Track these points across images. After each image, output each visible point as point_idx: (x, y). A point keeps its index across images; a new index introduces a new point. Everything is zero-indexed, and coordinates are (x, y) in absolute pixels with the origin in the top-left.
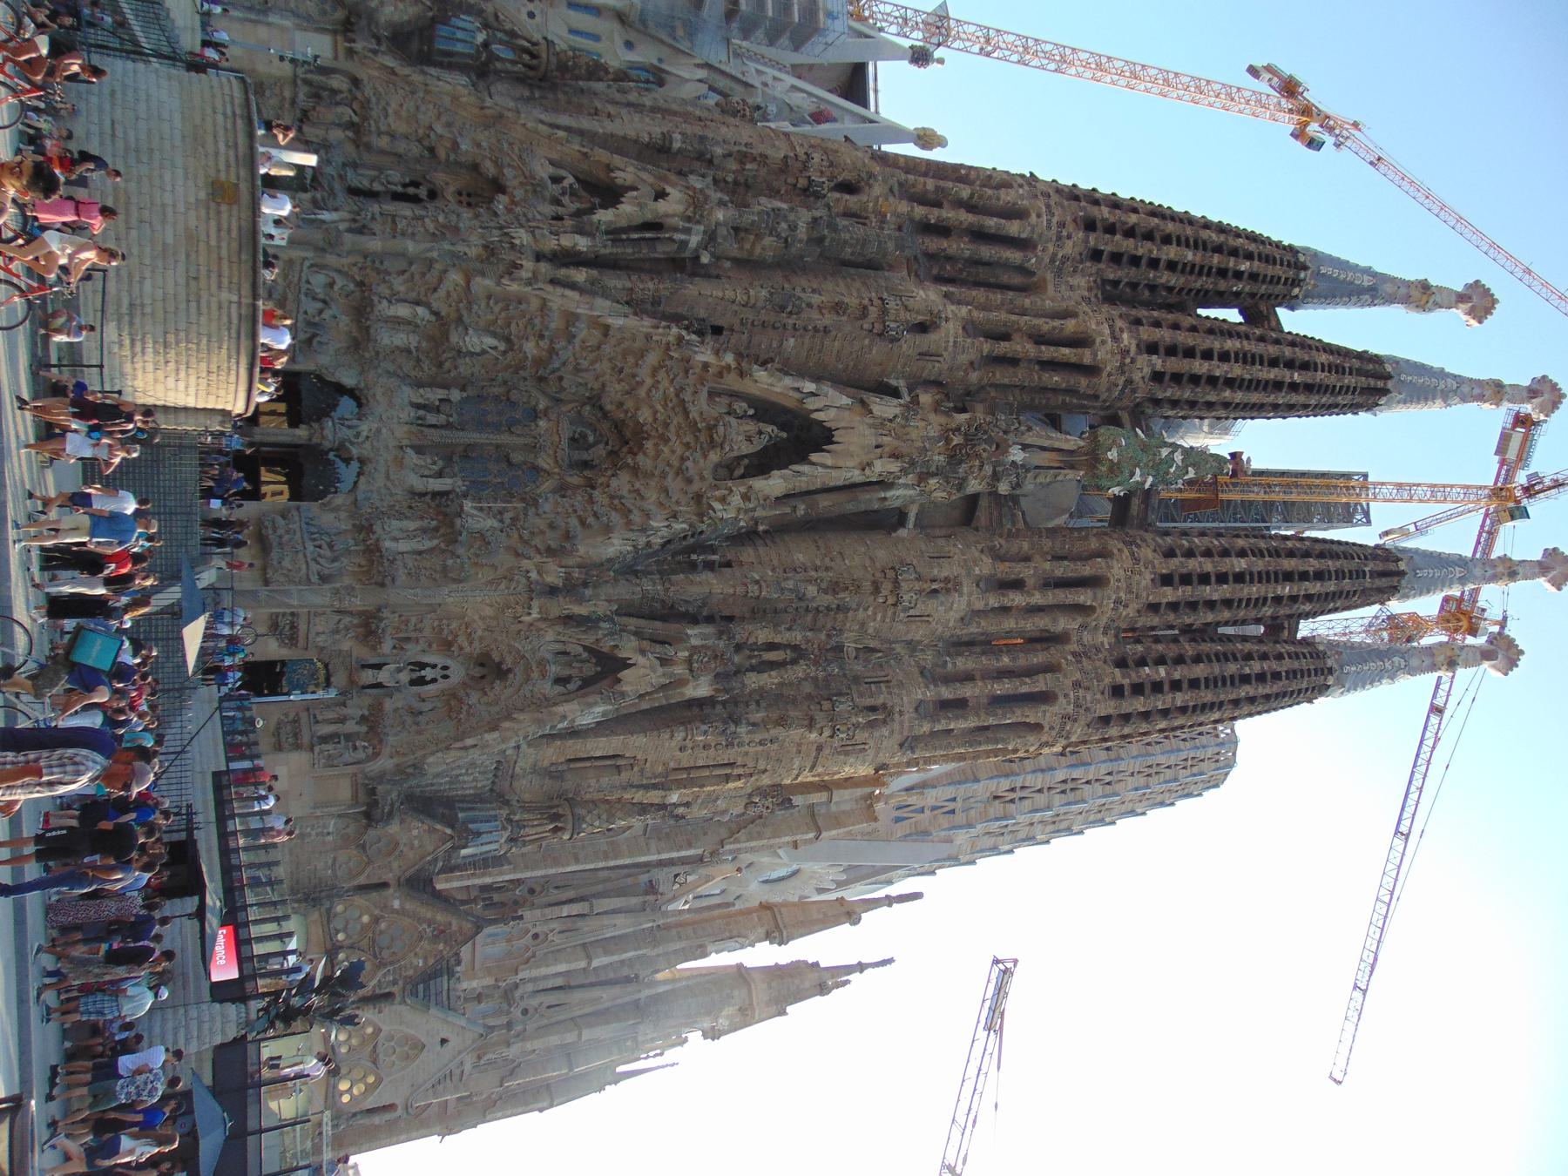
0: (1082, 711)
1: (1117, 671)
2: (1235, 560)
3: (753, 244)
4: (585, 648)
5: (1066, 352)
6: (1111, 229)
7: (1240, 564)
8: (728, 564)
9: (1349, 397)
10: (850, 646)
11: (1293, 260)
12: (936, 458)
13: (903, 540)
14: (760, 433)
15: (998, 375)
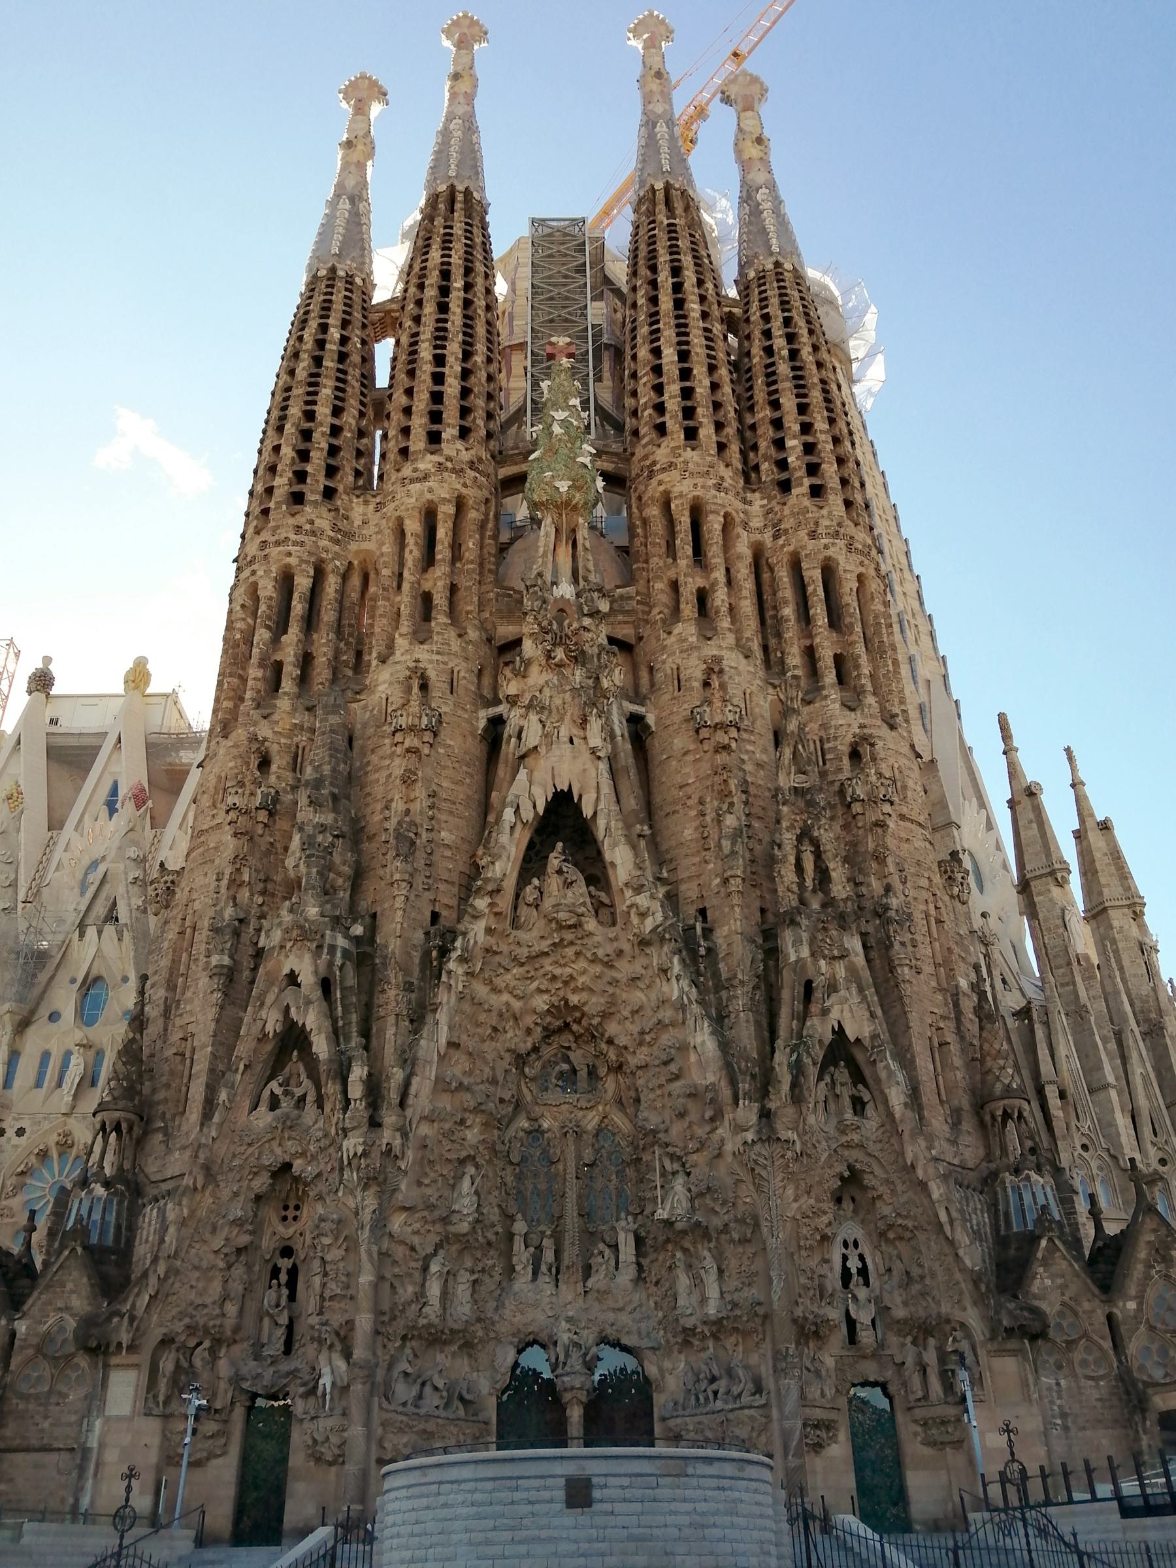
0: (842, 531)
1: (795, 491)
2: (664, 361)
3: (339, 874)
4: (820, 1078)
5: (443, 532)
6: (301, 476)
7: (669, 355)
8: (703, 912)
9: (475, 230)
10: (796, 780)
11: (325, 282)
12: (578, 678)
13: (659, 719)
14: (560, 872)
15: (469, 608)
